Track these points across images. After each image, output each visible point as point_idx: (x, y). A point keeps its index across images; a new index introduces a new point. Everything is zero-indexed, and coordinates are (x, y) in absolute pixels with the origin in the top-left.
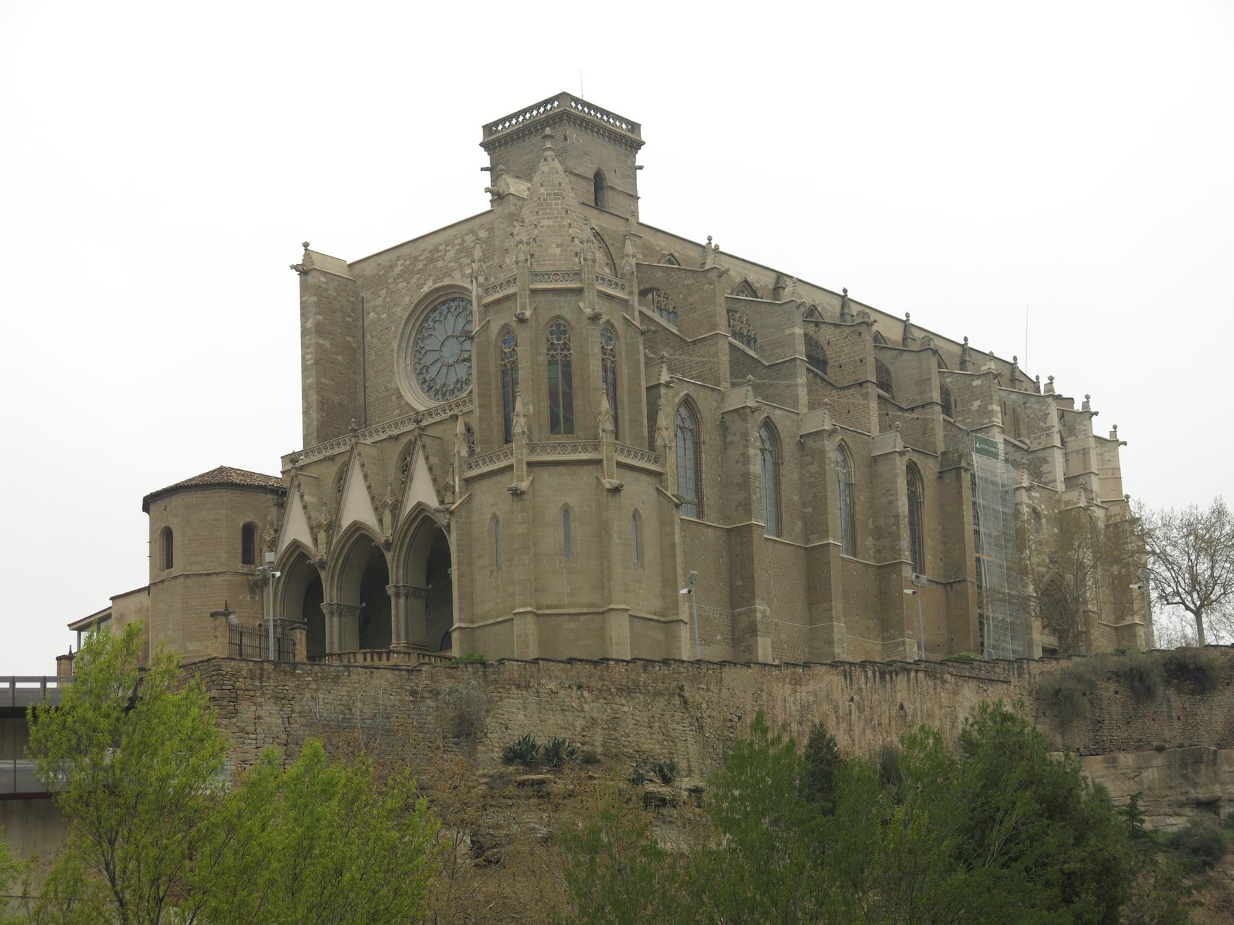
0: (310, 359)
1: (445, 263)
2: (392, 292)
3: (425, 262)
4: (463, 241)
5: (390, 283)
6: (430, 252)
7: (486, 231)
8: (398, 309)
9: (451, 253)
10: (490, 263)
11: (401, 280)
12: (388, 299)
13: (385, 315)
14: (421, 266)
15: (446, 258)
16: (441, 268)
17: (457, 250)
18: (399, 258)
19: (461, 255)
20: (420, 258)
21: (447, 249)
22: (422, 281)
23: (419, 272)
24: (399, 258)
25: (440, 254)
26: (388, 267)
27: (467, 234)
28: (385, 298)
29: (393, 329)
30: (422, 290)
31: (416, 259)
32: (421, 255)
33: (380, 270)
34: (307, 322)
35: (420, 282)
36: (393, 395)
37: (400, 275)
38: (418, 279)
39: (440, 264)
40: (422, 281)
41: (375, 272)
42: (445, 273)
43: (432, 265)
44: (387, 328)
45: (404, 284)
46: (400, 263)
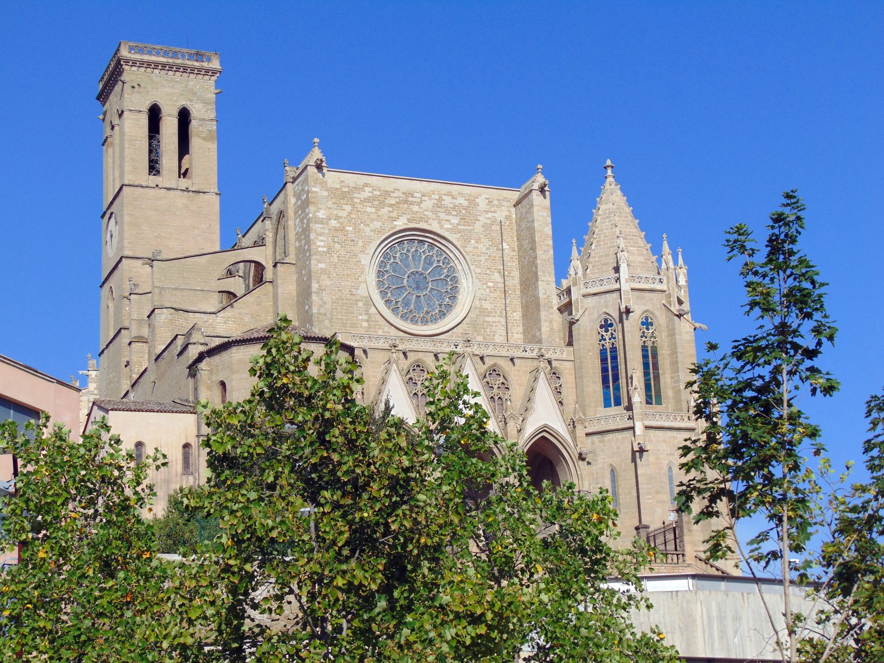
0: (322, 247)
1: (421, 210)
2: (358, 211)
3: (398, 200)
4: (440, 199)
5: (356, 203)
6: (403, 193)
7: (466, 200)
8: (367, 229)
9: (428, 204)
10: (470, 228)
11: (370, 204)
13: (350, 229)
14: (393, 202)
15: (422, 205)
16: (417, 212)
17: (434, 204)
18: (366, 185)
19: (439, 210)
20: (392, 194)
21: (423, 198)
22: (394, 214)
23: (391, 205)
24: (366, 185)
25: (414, 199)
26: (353, 187)
27: (445, 195)
28: (350, 213)
29: (361, 244)
30: (395, 223)
31: (387, 194)
32: (394, 192)
33: (344, 187)
34: (318, 212)
35: (392, 215)
36: (359, 301)
37: (367, 200)
38: (390, 212)
39: (415, 208)
40: (394, 214)
42: (421, 218)
43: (406, 206)
44: (353, 241)
45: (373, 210)
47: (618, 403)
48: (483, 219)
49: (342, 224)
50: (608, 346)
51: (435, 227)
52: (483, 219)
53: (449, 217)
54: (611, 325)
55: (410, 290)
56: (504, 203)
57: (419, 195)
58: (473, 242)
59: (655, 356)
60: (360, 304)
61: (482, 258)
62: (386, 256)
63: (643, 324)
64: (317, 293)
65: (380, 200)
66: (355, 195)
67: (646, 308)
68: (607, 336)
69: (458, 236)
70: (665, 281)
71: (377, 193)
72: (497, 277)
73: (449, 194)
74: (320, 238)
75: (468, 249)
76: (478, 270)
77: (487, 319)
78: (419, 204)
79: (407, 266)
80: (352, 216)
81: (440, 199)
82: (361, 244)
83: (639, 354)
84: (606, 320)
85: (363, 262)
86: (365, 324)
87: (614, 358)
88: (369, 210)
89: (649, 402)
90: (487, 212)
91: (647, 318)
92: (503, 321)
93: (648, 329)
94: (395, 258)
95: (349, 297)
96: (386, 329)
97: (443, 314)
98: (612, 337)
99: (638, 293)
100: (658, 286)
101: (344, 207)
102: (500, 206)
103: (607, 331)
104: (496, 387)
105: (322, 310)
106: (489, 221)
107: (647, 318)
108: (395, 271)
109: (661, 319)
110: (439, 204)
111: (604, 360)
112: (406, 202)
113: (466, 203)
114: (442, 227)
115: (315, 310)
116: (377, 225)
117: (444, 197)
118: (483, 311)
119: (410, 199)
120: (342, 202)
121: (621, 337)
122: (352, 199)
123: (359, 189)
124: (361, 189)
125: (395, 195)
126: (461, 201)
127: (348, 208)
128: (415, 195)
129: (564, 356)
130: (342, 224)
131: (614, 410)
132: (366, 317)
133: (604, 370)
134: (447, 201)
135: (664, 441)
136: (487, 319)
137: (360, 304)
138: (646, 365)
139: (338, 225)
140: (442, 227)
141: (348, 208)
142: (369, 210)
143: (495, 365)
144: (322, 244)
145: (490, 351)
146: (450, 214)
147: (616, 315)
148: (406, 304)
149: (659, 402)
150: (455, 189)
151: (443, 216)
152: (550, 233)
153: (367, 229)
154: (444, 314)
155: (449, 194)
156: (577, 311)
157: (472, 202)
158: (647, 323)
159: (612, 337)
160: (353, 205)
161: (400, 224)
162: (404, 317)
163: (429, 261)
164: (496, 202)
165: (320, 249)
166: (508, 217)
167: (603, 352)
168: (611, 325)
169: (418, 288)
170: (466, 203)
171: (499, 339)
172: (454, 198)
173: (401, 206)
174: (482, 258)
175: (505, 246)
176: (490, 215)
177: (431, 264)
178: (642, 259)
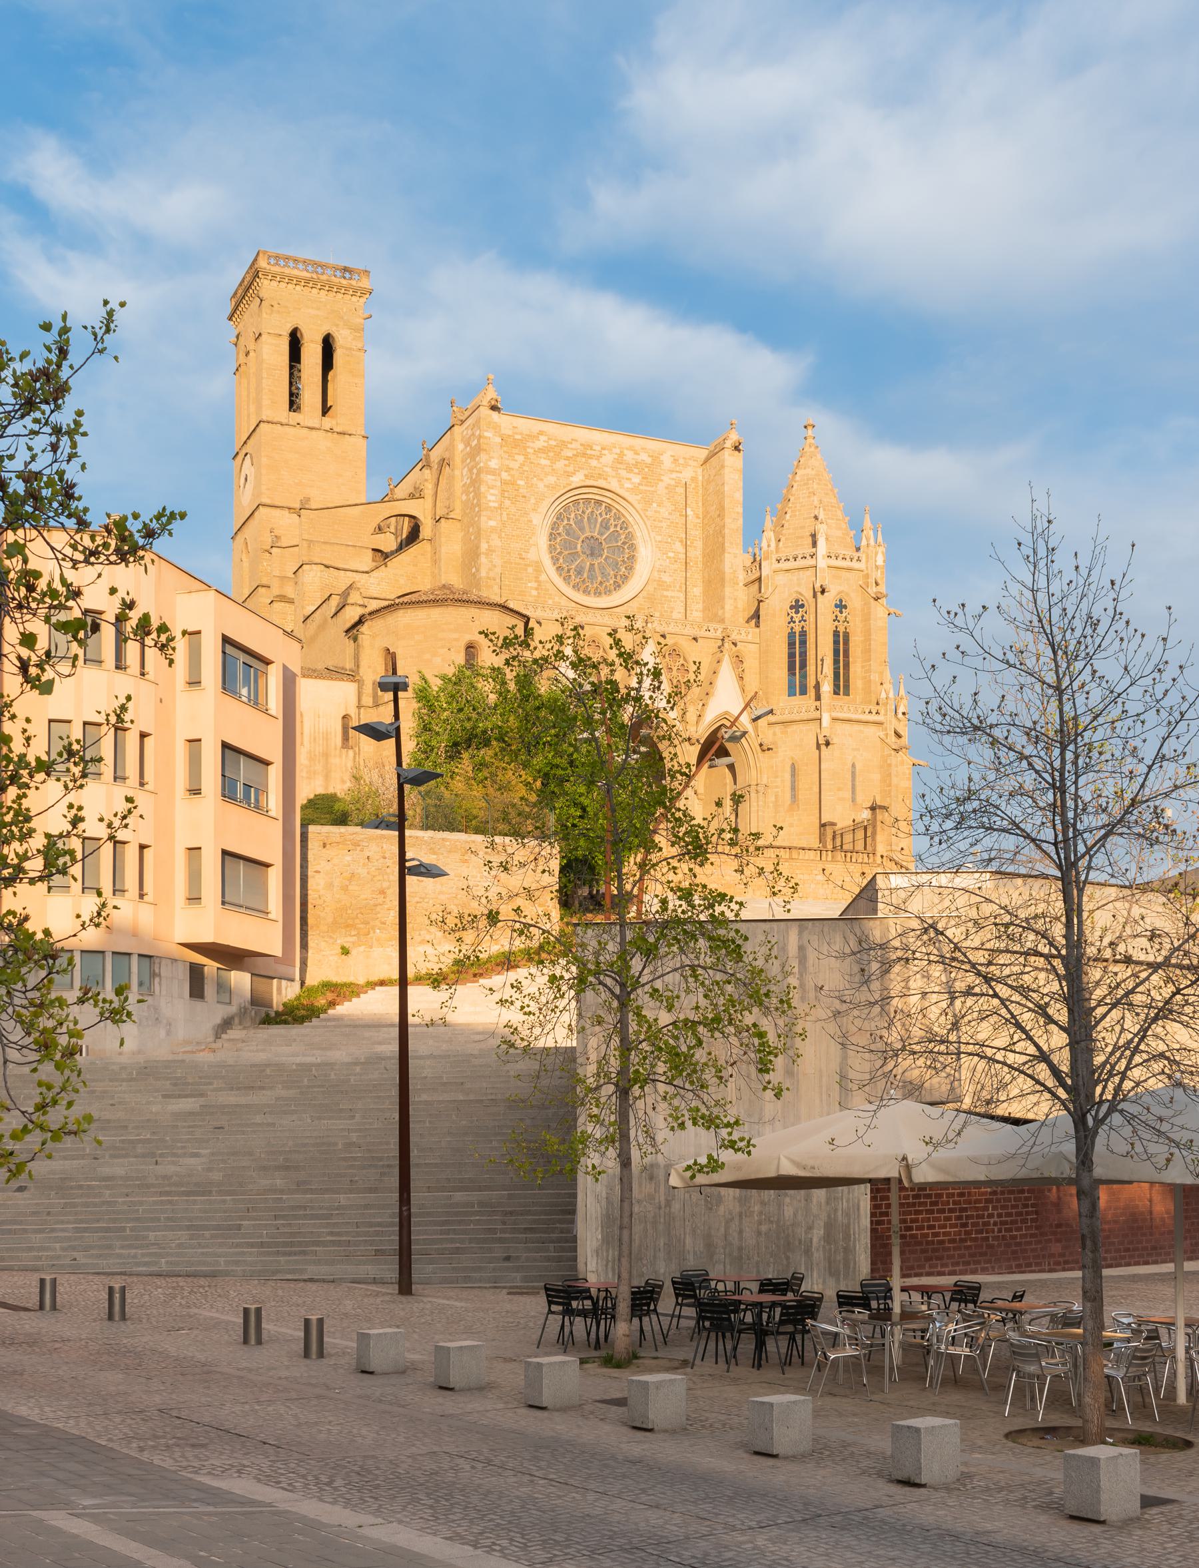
4: (621, 455)
8: (541, 485)
9: (608, 458)
12: (526, 468)
14: (570, 454)
22: (571, 469)
23: (567, 458)
24: (541, 433)
28: (522, 465)
29: (533, 501)
31: (563, 444)
35: (568, 469)
37: (542, 450)
39: (594, 463)
41: (510, 433)
45: (547, 462)
46: (542, 438)
47: (803, 691)
48: (667, 480)
49: (513, 476)
50: (797, 629)
51: (614, 485)
52: (667, 480)
53: (630, 476)
54: (803, 606)
55: (583, 557)
56: (691, 462)
57: (598, 448)
58: (655, 505)
59: (846, 642)
60: (530, 570)
61: (664, 525)
62: (559, 517)
63: (836, 606)
64: (487, 554)
65: (555, 450)
66: (529, 444)
67: (842, 588)
68: (797, 618)
69: (638, 497)
70: (864, 559)
71: (553, 443)
72: (679, 547)
73: (631, 448)
74: (492, 491)
75: (649, 513)
76: (659, 538)
77: (665, 593)
78: (598, 458)
79: (582, 529)
80: (526, 468)
81: (621, 455)
82: (533, 501)
83: (830, 639)
84: (797, 601)
85: (535, 522)
86: (534, 593)
87: (803, 643)
88: (544, 462)
89: (836, 693)
90: (672, 471)
91: (841, 601)
92: (682, 596)
93: (841, 612)
94: (569, 519)
95: (518, 561)
96: (557, 599)
97: (617, 586)
98: (803, 620)
99: (834, 571)
100: (855, 565)
101: (517, 457)
102: (686, 465)
103: (797, 612)
104: (675, 669)
105: (491, 574)
106: (673, 482)
107: (841, 601)
108: (568, 534)
109: (855, 602)
110: (620, 460)
111: (791, 645)
112: (584, 455)
113: (649, 460)
114: (622, 486)
115: (483, 573)
116: (551, 479)
117: (626, 452)
118: (661, 583)
119: (589, 452)
120: (515, 451)
121: (812, 619)
122: (525, 448)
123: (534, 437)
124: (535, 437)
125: (573, 446)
126: (644, 457)
127: (521, 458)
128: (595, 447)
129: (750, 638)
130: (513, 476)
131: (798, 700)
132: (535, 585)
133: (791, 656)
134: (629, 456)
135: (851, 735)
136: (665, 593)
137: (530, 570)
138: (836, 652)
139: (509, 478)
140: (622, 486)
141: (521, 458)
142: (544, 462)
143: (675, 644)
144: (493, 498)
145: (671, 629)
146: (630, 471)
147: (809, 594)
148: (579, 572)
149: (847, 693)
150: (638, 442)
151: (623, 473)
152: (741, 499)
153: (541, 485)
154: (619, 586)
155: (631, 448)
156: (767, 588)
157: (656, 458)
158: (841, 606)
159: (803, 620)
160: (526, 455)
161: (577, 479)
162: (576, 587)
163: (605, 526)
164: (681, 461)
165: (491, 504)
166: (694, 479)
167: (791, 635)
168: (803, 606)
169: (592, 554)
170: (649, 460)
171: (678, 614)
172: (637, 453)
173: (579, 459)
174: (664, 525)
175: (689, 512)
176: (674, 475)
177: (607, 528)
178: (839, 533)
